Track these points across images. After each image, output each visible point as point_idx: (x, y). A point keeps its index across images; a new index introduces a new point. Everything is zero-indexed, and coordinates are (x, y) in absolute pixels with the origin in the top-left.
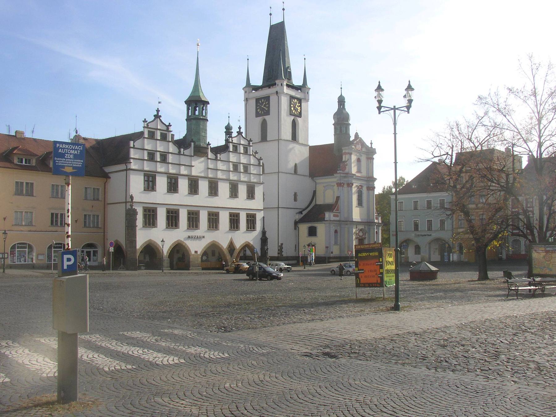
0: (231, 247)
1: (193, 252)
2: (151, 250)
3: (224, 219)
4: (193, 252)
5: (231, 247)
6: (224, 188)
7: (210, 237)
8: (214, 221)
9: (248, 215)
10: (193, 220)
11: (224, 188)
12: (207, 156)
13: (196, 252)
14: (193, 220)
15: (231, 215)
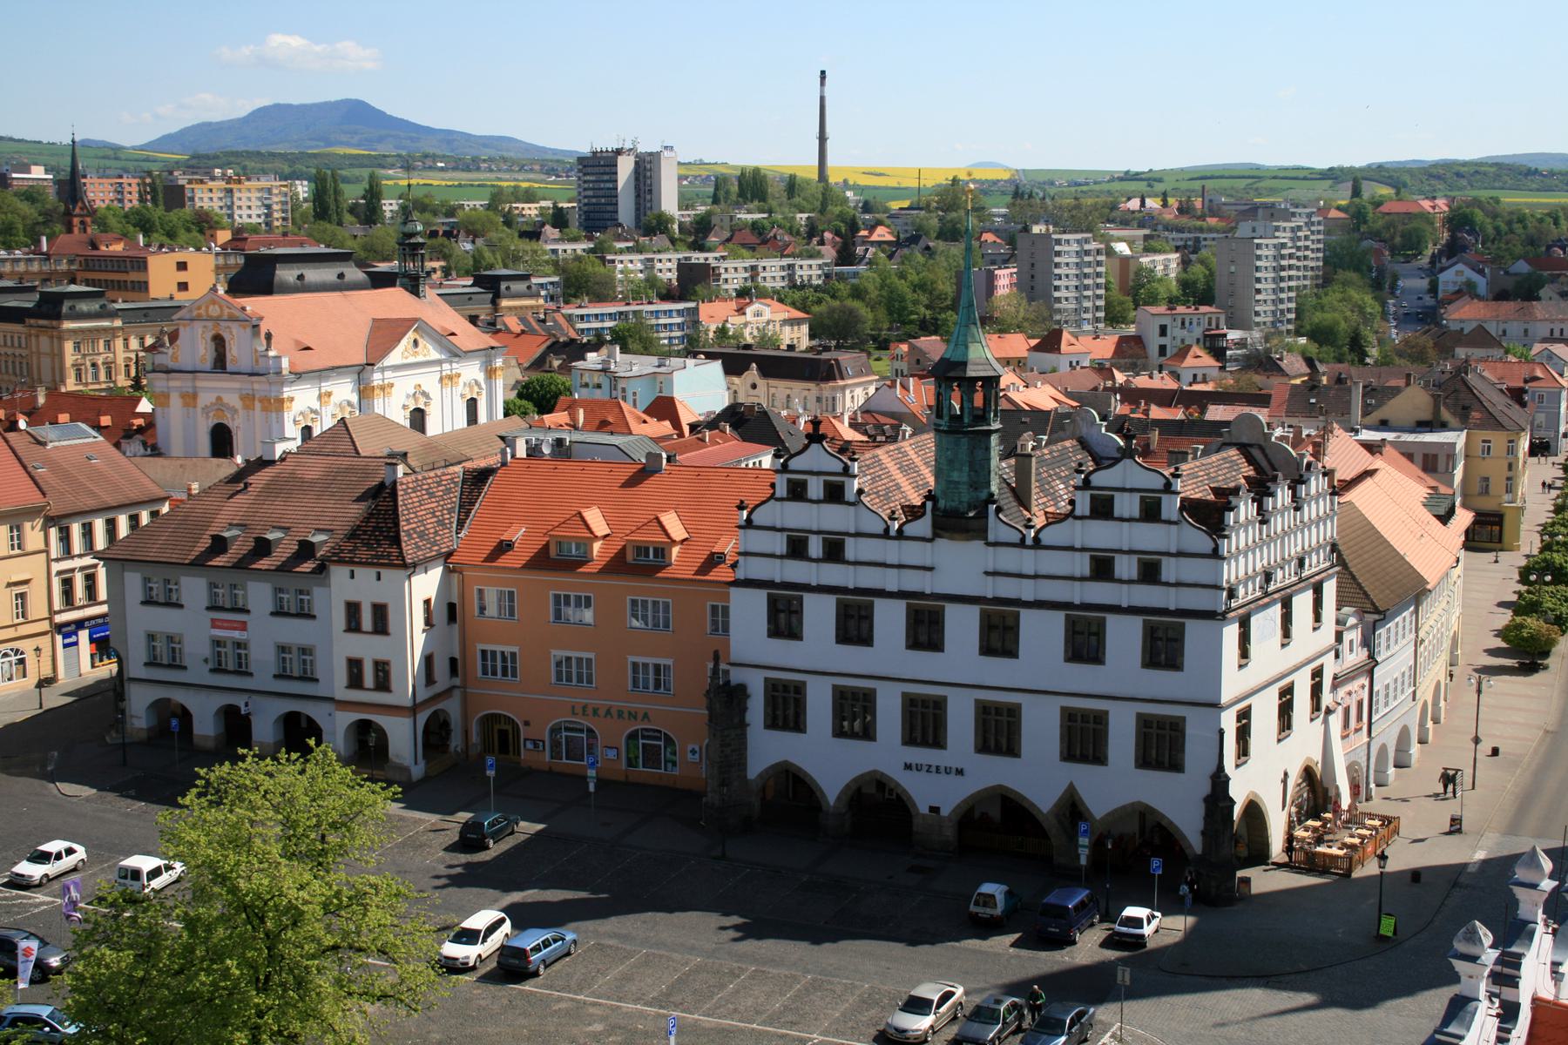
0: (1072, 808)
1: (923, 809)
2: (792, 784)
3: (1041, 727)
4: (923, 809)
5: (1072, 808)
6: (1042, 635)
7: (993, 772)
8: (999, 730)
9: (1144, 722)
10: (924, 720)
11: (1042, 635)
12: (986, 538)
13: (935, 810)
14: (924, 720)
15: (1069, 716)
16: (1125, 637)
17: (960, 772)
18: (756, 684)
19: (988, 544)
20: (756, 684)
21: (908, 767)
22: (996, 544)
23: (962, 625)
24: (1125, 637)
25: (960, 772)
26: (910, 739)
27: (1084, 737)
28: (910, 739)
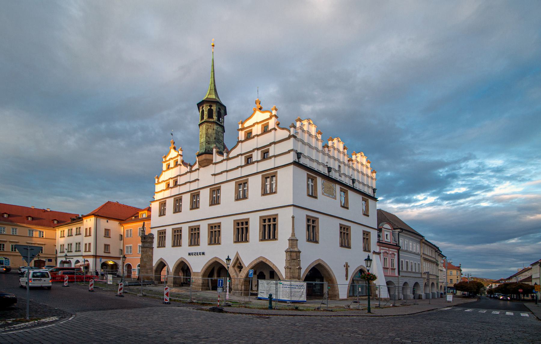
6: (228, 192)
9: (263, 220)
11: (228, 192)
16: (255, 185)
17: (203, 254)
18: (155, 232)
19: (213, 164)
20: (155, 232)
21: (189, 254)
22: (216, 164)
23: (205, 196)
24: (255, 185)
25: (203, 254)
26: (191, 245)
27: (241, 231)
28: (191, 245)
